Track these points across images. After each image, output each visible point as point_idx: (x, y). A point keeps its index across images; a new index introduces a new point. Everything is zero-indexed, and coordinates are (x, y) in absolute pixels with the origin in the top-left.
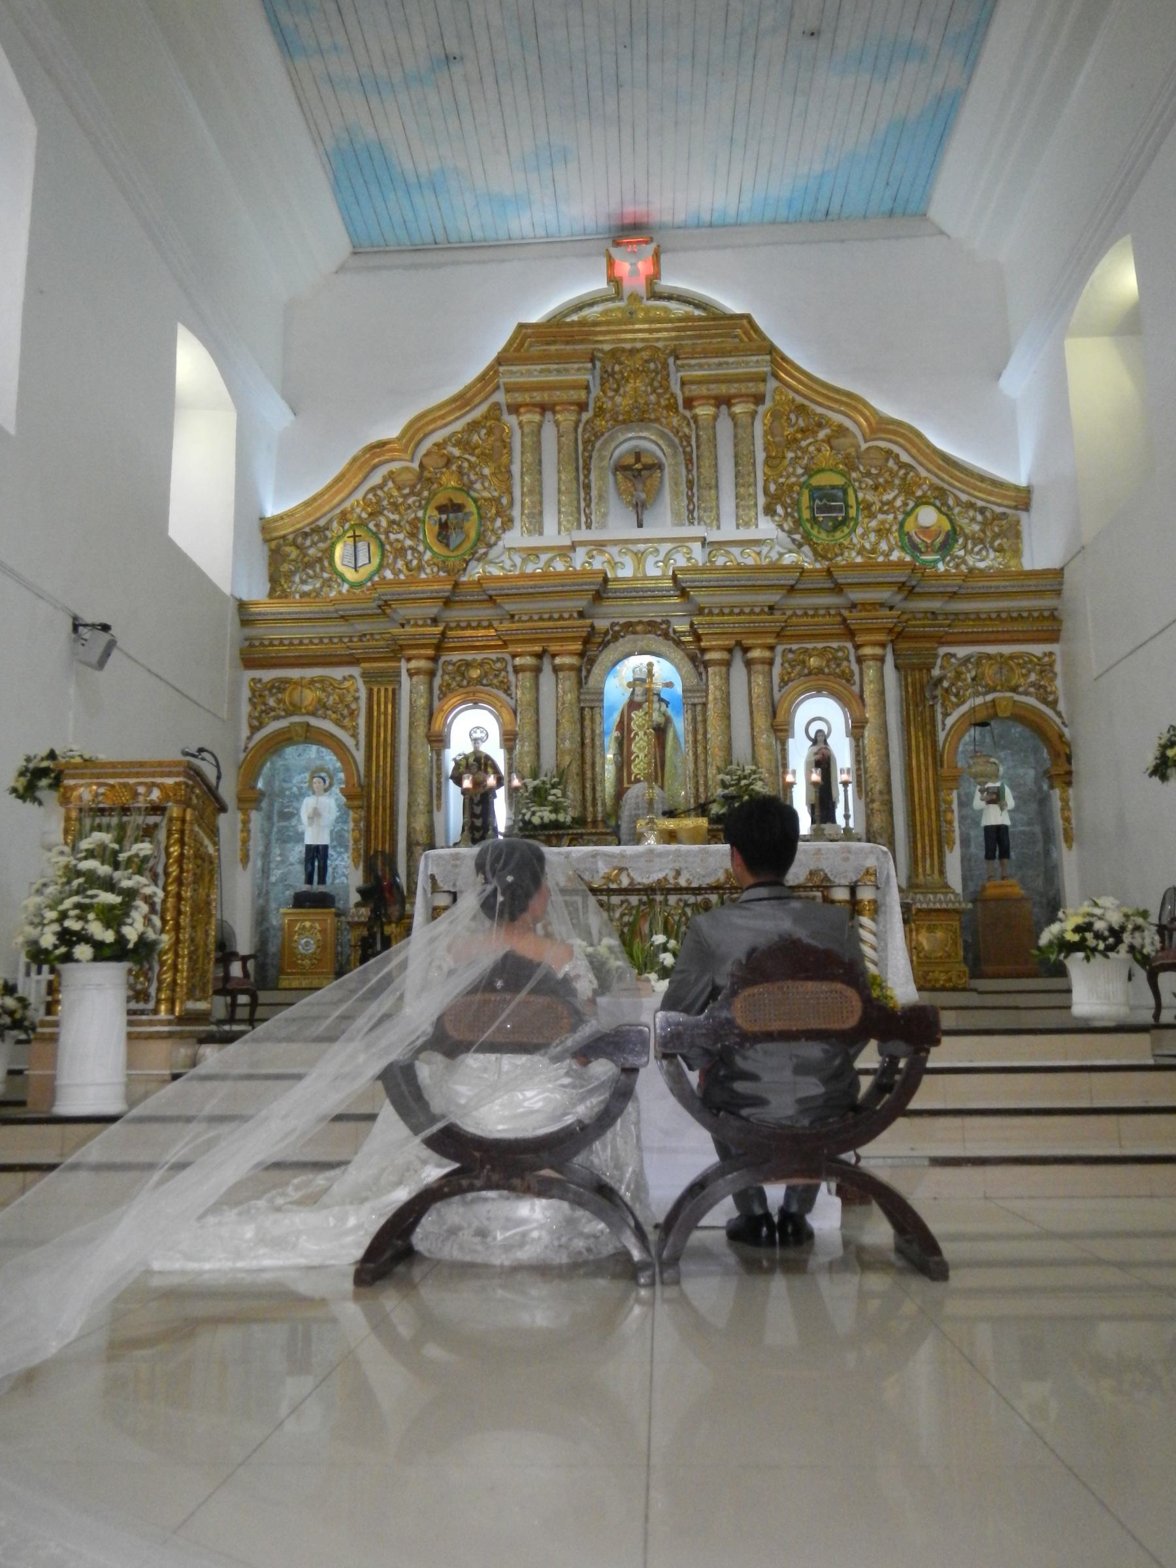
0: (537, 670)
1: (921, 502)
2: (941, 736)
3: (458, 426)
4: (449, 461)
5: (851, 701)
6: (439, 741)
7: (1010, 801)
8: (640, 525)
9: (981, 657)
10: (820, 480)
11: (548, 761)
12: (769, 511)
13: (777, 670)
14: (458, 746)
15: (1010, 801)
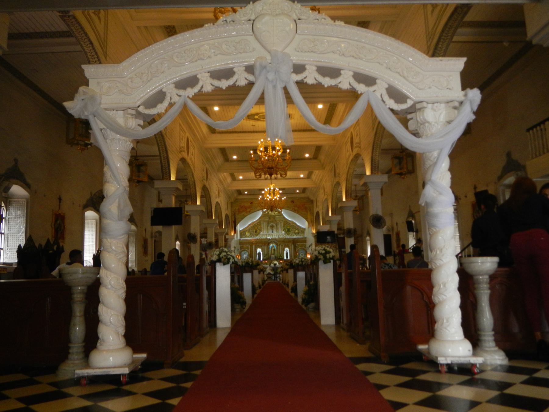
0: (264, 246)
1: (297, 230)
2: (297, 251)
3: (257, 222)
4: (256, 225)
5: (289, 248)
6: (256, 251)
7: (303, 255)
8: (273, 232)
9: (300, 244)
10: (287, 228)
11: (265, 253)
12: (283, 230)
13: (283, 245)
14: (258, 252)
15: (303, 255)
